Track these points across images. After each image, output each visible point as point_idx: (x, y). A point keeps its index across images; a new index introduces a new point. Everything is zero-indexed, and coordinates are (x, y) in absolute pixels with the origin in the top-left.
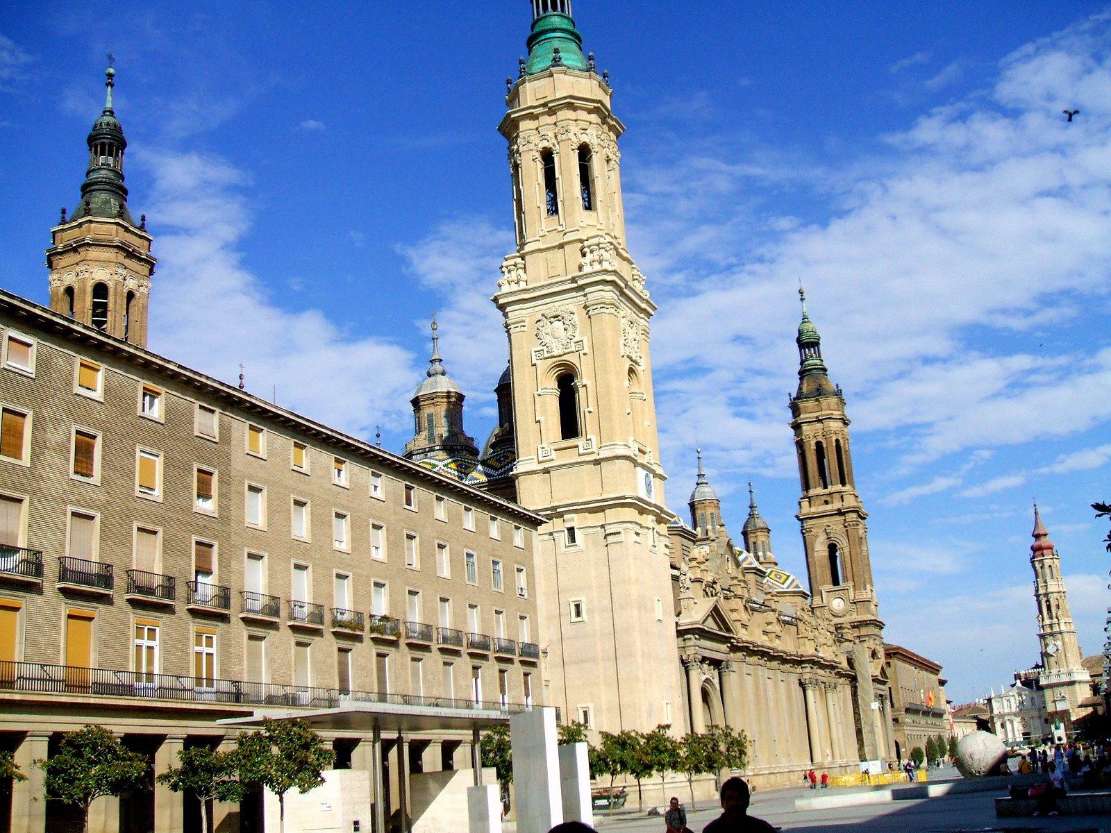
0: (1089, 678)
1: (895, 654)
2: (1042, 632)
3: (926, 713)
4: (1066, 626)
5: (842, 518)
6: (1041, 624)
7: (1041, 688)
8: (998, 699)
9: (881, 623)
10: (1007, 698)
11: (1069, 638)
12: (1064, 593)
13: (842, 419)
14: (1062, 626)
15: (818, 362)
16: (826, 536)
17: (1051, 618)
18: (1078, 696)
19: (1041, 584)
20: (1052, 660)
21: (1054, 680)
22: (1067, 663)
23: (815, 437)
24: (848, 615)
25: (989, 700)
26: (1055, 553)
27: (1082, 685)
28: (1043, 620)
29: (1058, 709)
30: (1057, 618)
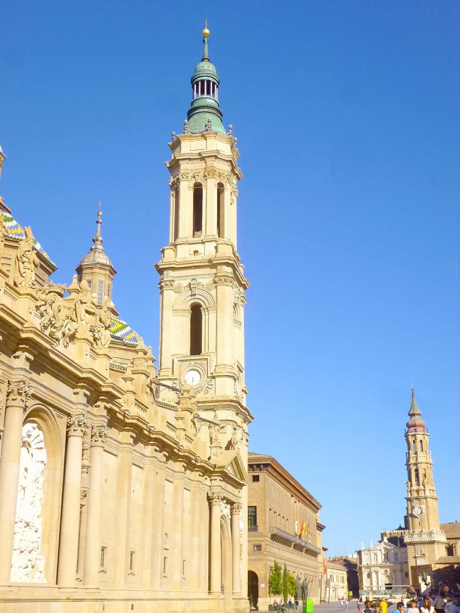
0: (446, 540)
1: (266, 465)
2: (410, 496)
3: (299, 547)
4: (430, 493)
5: (214, 271)
6: (409, 490)
7: (404, 545)
8: (367, 552)
9: (248, 411)
10: (375, 552)
11: (432, 504)
12: (430, 464)
13: (230, 161)
14: (427, 492)
15: (213, 102)
16: (190, 292)
17: (418, 485)
18: (436, 555)
19: (412, 455)
20: (417, 521)
21: (416, 539)
22: (428, 524)
23: (194, 177)
24: (203, 392)
25: (359, 553)
26: (426, 430)
27: (440, 545)
28: (411, 486)
29: (418, 565)
30: (424, 486)
